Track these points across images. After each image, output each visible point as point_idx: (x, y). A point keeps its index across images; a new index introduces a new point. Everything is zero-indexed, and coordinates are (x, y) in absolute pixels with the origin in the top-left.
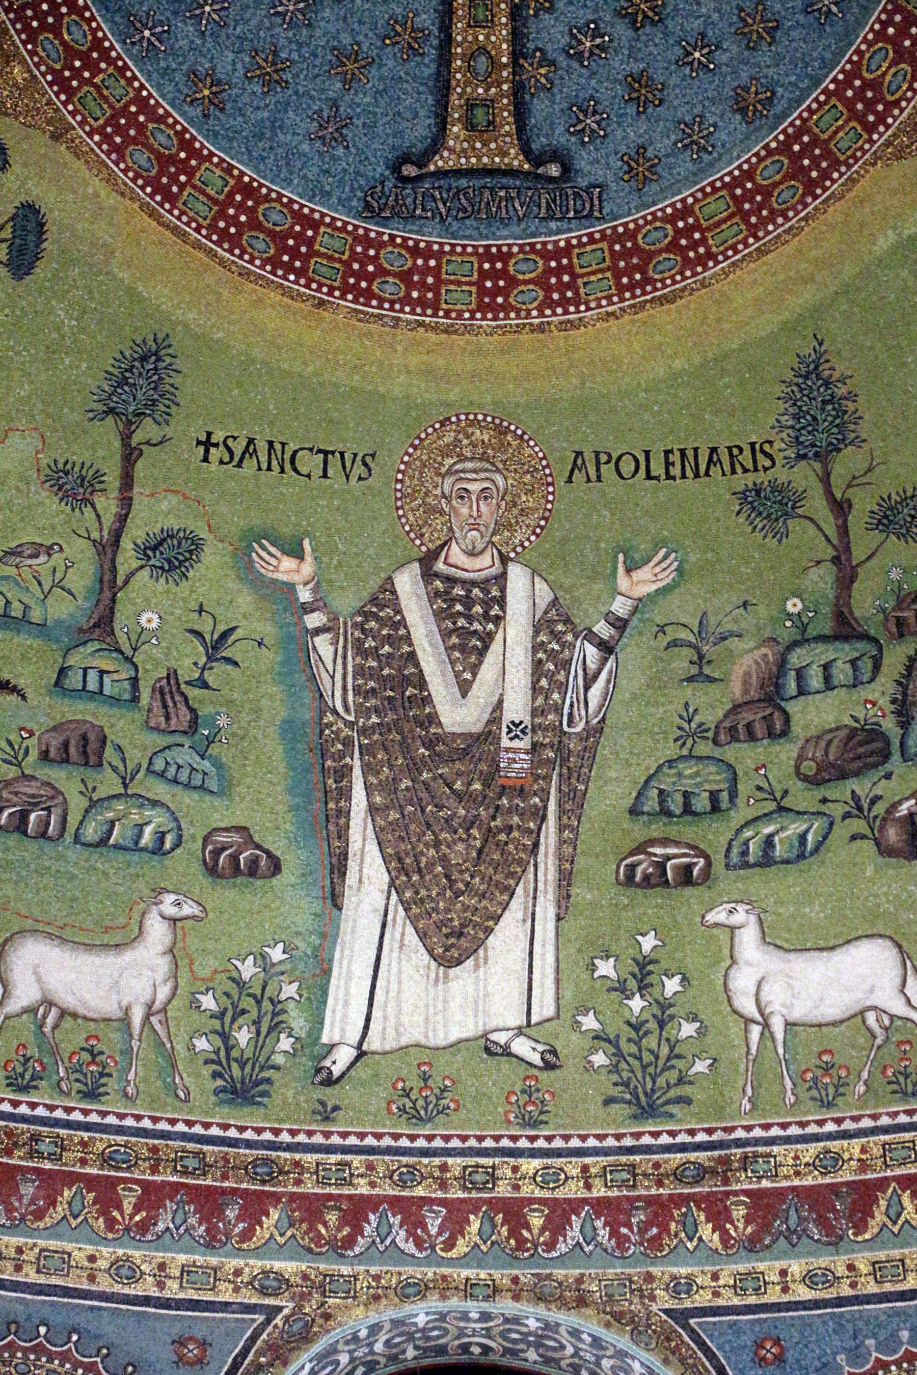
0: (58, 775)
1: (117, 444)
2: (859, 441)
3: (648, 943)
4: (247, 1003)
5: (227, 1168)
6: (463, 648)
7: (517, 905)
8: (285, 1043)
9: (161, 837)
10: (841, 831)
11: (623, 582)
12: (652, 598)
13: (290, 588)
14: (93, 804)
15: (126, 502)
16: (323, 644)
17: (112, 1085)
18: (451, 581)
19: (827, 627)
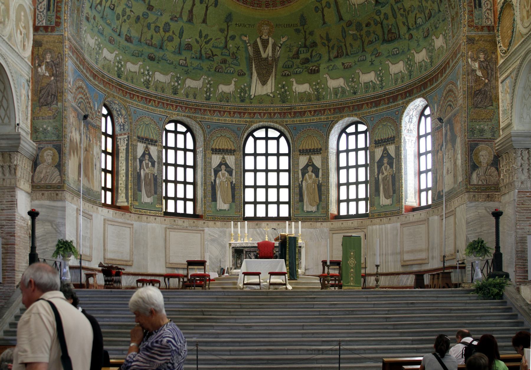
0: (222, 65)
1: (226, 25)
2: (307, 24)
3: (284, 83)
4: (243, 90)
5: (241, 109)
6: (265, 48)
7: (270, 78)
8: (247, 95)
9: (233, 71)
10: (304, 70)
11: (282, 40)
12: (285, 42)
13: (246, 41)
14: (226, 68)
15: (228, 32)
16: (249, 48)
17: (229, 101)
18: (263, 39)
19: (303, 46)
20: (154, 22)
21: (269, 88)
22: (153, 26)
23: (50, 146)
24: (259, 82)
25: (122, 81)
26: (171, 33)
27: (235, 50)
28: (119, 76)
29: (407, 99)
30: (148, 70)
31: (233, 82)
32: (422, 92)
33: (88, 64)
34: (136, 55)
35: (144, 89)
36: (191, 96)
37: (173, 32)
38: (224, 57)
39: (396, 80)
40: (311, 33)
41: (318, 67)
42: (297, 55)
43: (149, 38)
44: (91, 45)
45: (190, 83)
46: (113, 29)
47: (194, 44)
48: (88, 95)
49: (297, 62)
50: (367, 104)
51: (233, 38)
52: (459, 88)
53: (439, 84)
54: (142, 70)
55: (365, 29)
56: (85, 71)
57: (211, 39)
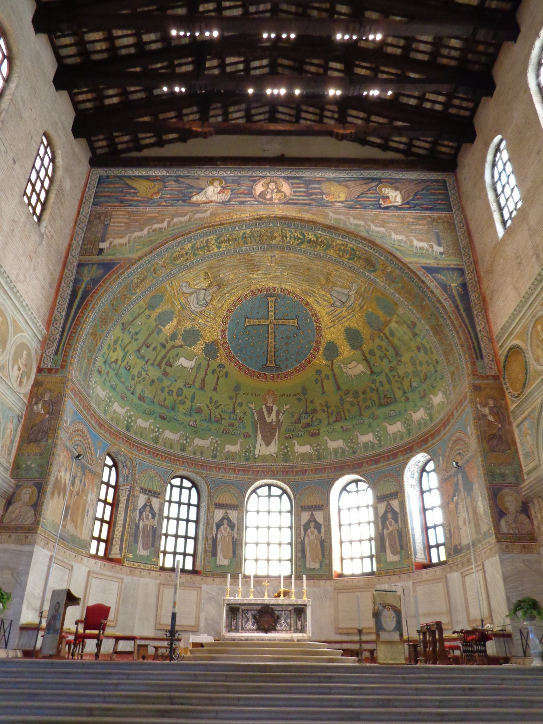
20: (168, 387)
21: (272, 449)
22: (166, 390)
23: (30, 484)
24: (263, 443)
25: (131, 434)
26: (183, 397)
27: (242, 415)
28: (128, 429)
29: (408, 455)
30: (158, 428)
31: (239, 443)
32: (424, 447)
33: (95, 412)
34: (148, 414)
35: (153, 444)
36: (198, 453)
37: (186, 397)
38: (231, 421)
39: (395, 439)
40: (312, 402)
41: (319, 430)
42: (299, 421)
43: (162, 399)
44: (101, 396)
45: (198, 442)
46: (127, 388)
47: (205, 408)
48: (89, 440)
49: (299, 426)
50: (367, 462)
51: (241, 405)
52: (470, 434)
53: (442, 437)
54: (152, 427)
55: (362, 396)
56: (89, 417)
57: (221, 405)
